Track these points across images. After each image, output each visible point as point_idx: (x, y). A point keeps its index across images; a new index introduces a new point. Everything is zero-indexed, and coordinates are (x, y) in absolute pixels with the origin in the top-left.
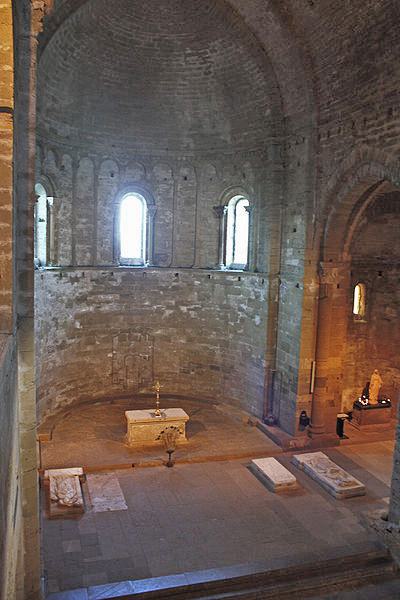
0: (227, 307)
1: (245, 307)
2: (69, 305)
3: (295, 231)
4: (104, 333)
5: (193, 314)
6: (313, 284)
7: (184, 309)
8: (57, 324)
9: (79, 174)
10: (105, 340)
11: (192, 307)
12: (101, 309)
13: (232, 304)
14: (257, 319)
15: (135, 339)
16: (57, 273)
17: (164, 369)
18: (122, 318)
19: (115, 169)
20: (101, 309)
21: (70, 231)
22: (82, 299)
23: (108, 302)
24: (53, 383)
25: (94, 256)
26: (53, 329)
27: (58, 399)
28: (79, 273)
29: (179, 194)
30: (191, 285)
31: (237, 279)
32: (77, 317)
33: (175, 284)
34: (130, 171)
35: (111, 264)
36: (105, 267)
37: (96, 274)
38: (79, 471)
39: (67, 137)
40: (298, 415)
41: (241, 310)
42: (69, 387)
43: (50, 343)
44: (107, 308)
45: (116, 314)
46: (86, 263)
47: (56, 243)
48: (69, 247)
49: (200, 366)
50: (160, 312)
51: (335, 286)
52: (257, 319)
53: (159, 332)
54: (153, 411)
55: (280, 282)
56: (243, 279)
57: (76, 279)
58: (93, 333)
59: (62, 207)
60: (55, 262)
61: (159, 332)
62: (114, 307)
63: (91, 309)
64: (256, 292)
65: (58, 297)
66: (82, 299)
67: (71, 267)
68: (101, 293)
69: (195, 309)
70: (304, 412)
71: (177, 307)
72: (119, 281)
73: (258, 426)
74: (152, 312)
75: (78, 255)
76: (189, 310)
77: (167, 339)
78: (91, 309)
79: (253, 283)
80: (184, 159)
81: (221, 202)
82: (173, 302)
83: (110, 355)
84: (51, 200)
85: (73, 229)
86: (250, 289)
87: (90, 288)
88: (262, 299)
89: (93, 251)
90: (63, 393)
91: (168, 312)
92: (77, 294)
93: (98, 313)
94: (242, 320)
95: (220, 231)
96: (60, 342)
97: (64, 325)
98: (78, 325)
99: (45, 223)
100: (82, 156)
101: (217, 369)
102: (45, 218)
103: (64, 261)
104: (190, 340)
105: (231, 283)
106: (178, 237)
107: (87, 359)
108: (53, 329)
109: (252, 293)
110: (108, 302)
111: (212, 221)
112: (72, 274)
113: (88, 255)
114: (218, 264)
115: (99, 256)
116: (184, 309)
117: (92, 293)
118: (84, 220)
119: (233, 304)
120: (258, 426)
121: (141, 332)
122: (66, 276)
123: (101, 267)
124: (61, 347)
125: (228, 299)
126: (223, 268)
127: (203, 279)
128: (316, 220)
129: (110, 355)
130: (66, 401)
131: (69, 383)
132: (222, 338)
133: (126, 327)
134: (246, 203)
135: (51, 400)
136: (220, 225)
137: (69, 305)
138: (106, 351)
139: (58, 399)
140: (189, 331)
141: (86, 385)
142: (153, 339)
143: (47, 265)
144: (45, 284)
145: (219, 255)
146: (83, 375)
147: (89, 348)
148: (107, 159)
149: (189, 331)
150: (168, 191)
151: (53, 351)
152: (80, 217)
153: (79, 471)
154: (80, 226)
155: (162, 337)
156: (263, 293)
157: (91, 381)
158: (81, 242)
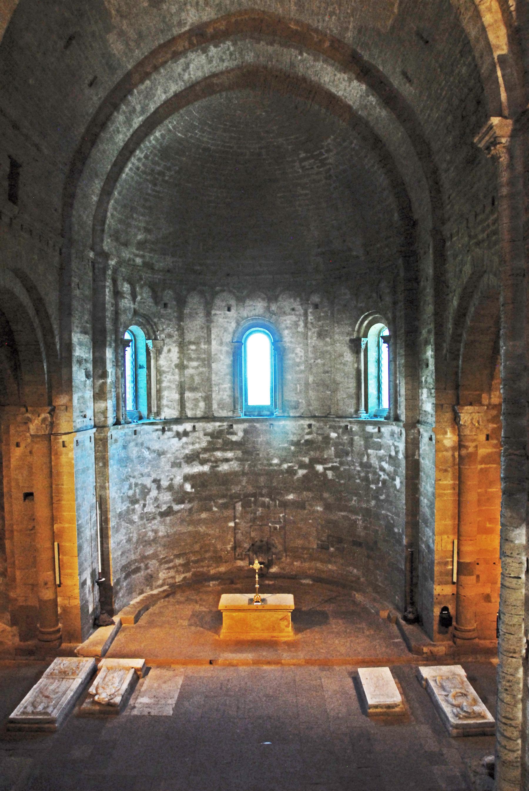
0: (367, 466)
1: (385, 465)
2: (176, 465)
3: (427, 366)
4: (224, 496)
5: (330, 474)
6: (449, 435)
7: (320, 468)
8: (159, 487)
9: (187, 311)
10: (225, 506)
11: (330, 465)
12: (220, 469)
13: (372, 462)
14: (398, 482)
15: (263, 505)
16: (160, 427)
17: (299, 542)
18: (245, 479)
19: (233, 302)
20: (220, 469)
21: (177, 377)
22: (190, 459)
23: (227, 460)
24: (155, 556)
25: (209, 406)
26: (154, 493)
27: (162, 575)
28: (188, 426)
29: (310, 326)
30: (327, 438)
31: (376, 430)
32: (187, 478)
33: (308, 437)
34: (251, 303)
35: (230, 414)
36: (221, 419)
37: (211, 427)
38: (139, 663)
39: (168, 271)
40: (437, 611)
41: (382, 469)
42: (178, 561)
43: (150, 508)
44: (224, 467)
45: (234, 474)
46: (199, 413)
47: (159, 391)
48: (177, 397)
49: (340, 540)
50: (291, 472)
51: (482, 437)
52: (398, 482)
53: (291, 497)
54: (252, 596)
55: (419, 432)
56: (382, 430)
57: (186, 434)
58: (210, 498)
59: (165, 349)
60: (158, 414)
61: (291, 497)
62: (235, 466)
63: (206, 468)
64: (396, 447)
65: (160, 454)
66: (190, 459)
67: (178, 421)
68: (218, 449)
69: (332, 469)
70: (445, 609)
71: (310, 466)
72: (241, 434)
73: (397, 623)
74: (282, 472)
75: (189, 405)
76: (325, 469)
77: (300, 505)
78: (206, 468)
79: (392, 434)
80: (314, 283)
81: (359, 331)
82: (306, 460)
83: (232, 524)
84: (150, 342)
85: (181, 374)
86: (390, 442)
87: (204, 444)
88: (401, 456)
89: (208, 399)
90: (169, 568)
91: (301, 472)
92: (187, 451)
93: (214, 473)
94: (384, 482)
95: (358, 371)
96: (164, 508)
97: (170, 488)
98: (188, 487)
99: (145, 370)
100: (189, 291)
101: (360, 545)
102: (145, 366)
103: (169, 413)
104: (328, 507)
105: (371, 435)
106: (311, 379)
107: (202, 529)
108: (154, 493)
109: (393, 448)
110: (227, 460)
111: (349, 357)
112: (180, 428)
113: (202, 404)
114: (357, 411)
115: (215, 406)
116: (320, 468)
117: (205, 450)
118: (195, 364)
119: (374, 461)
120: (397, 623)
121: (269, 495)
122: (170, 430)
123: (214, 419)
124: (163, 515)
125: (368, 456)
126: (363, 416)
127: (341, 430)
128: (447, 351)
129: (232, 524)
130: (173, 577)
131: (178, 556)
132: (364, 506)
133: (250, 489)
134: (386, 333)
135: (151, 576)
136: (358, 361)
137: (176, 465)
138: (227, 519)
139: (162, 575)
140: (326, 495)
141: (202, 560)
142: (285, 505)
143: (148, 418)
144: (140, 441)
145: (358, 398)
146: (197, 547)
147: (204, 515)
148: (223, 291)
149: (326, 495)
150: (296, 325)
151: (154, 518)
152: (190, 359)
153: (139, 663)
154: (189, 372)
155: (293, 503)
156: (402, 446)
157: (208, 555)
158: (193, 389)
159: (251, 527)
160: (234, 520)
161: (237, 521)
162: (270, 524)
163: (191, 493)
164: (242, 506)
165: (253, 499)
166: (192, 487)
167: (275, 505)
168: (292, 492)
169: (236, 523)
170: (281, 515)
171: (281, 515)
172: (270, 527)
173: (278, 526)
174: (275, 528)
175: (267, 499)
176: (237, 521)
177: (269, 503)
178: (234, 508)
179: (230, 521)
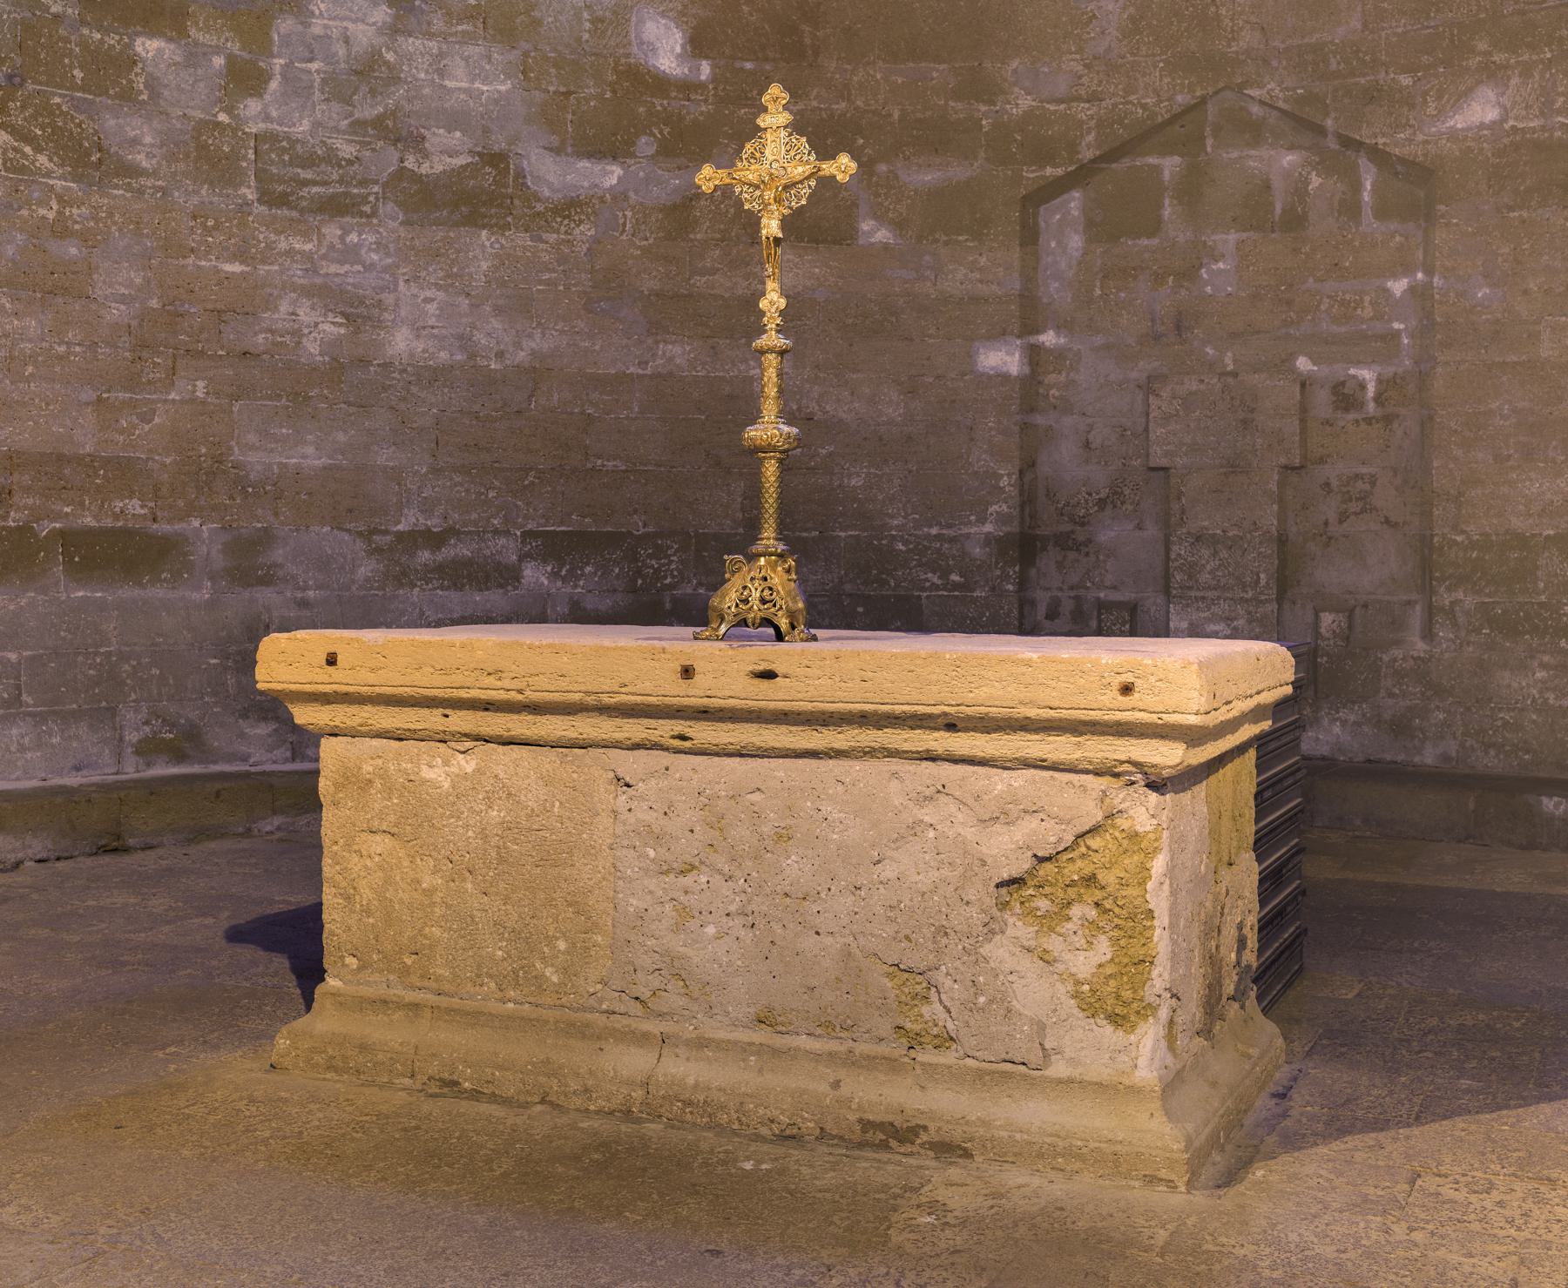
83: (1002, 359)
129: (1002, 359)
159: (1149, 386)
160: (1029, 327)
161: (1049, 338)
162: (1303, 364)
163: (687, 87)
164: (1095, 229)
165: (1170, 166)
166: (698, 45)
167: (1351, 209)
168: (1492, 73)
169: (1034, 355)
170: (1398, 286)
171: (1398, 286)
172: (1305, 384)
173: (1367, 375)
174: (1346, 397)
175: (1289, 159)
176: (1049, 338)
177: (1299, 190)
178: (1030, 236)
179: (997, 335)
